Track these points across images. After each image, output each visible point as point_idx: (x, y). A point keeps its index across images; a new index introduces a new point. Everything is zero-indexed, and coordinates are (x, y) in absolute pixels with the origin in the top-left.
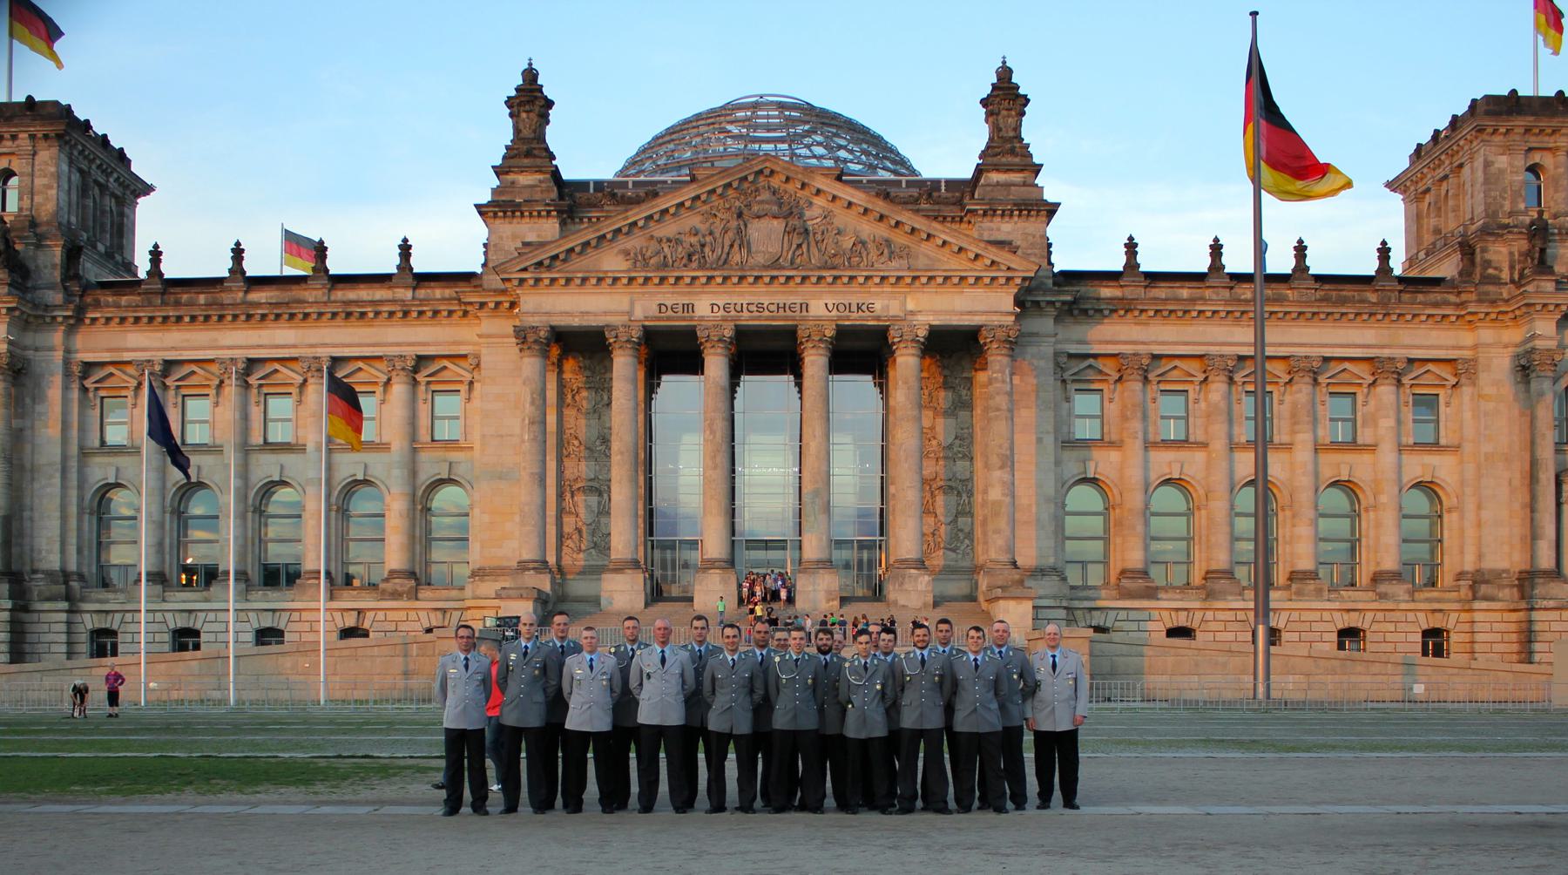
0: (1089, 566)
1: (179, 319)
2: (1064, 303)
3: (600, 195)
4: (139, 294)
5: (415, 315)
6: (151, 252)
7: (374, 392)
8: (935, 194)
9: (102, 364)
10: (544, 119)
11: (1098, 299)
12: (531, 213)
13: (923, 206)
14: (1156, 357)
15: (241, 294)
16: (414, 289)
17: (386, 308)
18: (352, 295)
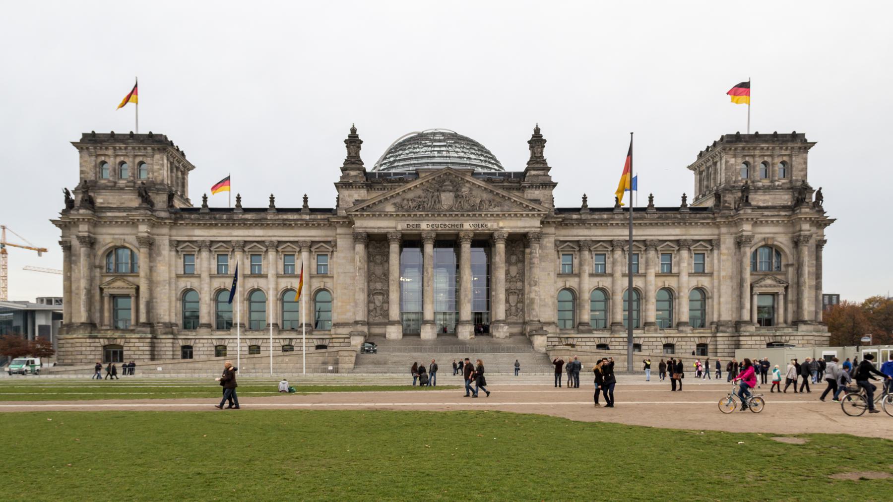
0: (567, 322)
1: (216, 225)
2: (559, 222)
3: (381, 179)
4: (199, 214)
5: (310, 225)
6: (203, 197)
7: (294, 255)
8: (510, 179)
9: (185, 242)
10: (359, 148)
11: (572, 219)
12: (356, 187)
13: (505, 184)
14: (593, 241)
15: (240, 216)
16: (310, 215)
17: (299, 223)
18: (285, 217)
